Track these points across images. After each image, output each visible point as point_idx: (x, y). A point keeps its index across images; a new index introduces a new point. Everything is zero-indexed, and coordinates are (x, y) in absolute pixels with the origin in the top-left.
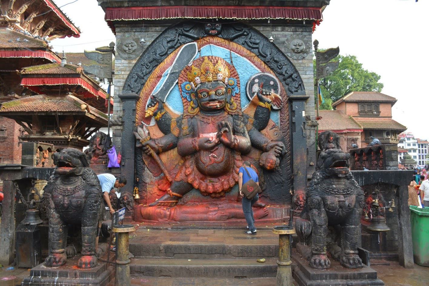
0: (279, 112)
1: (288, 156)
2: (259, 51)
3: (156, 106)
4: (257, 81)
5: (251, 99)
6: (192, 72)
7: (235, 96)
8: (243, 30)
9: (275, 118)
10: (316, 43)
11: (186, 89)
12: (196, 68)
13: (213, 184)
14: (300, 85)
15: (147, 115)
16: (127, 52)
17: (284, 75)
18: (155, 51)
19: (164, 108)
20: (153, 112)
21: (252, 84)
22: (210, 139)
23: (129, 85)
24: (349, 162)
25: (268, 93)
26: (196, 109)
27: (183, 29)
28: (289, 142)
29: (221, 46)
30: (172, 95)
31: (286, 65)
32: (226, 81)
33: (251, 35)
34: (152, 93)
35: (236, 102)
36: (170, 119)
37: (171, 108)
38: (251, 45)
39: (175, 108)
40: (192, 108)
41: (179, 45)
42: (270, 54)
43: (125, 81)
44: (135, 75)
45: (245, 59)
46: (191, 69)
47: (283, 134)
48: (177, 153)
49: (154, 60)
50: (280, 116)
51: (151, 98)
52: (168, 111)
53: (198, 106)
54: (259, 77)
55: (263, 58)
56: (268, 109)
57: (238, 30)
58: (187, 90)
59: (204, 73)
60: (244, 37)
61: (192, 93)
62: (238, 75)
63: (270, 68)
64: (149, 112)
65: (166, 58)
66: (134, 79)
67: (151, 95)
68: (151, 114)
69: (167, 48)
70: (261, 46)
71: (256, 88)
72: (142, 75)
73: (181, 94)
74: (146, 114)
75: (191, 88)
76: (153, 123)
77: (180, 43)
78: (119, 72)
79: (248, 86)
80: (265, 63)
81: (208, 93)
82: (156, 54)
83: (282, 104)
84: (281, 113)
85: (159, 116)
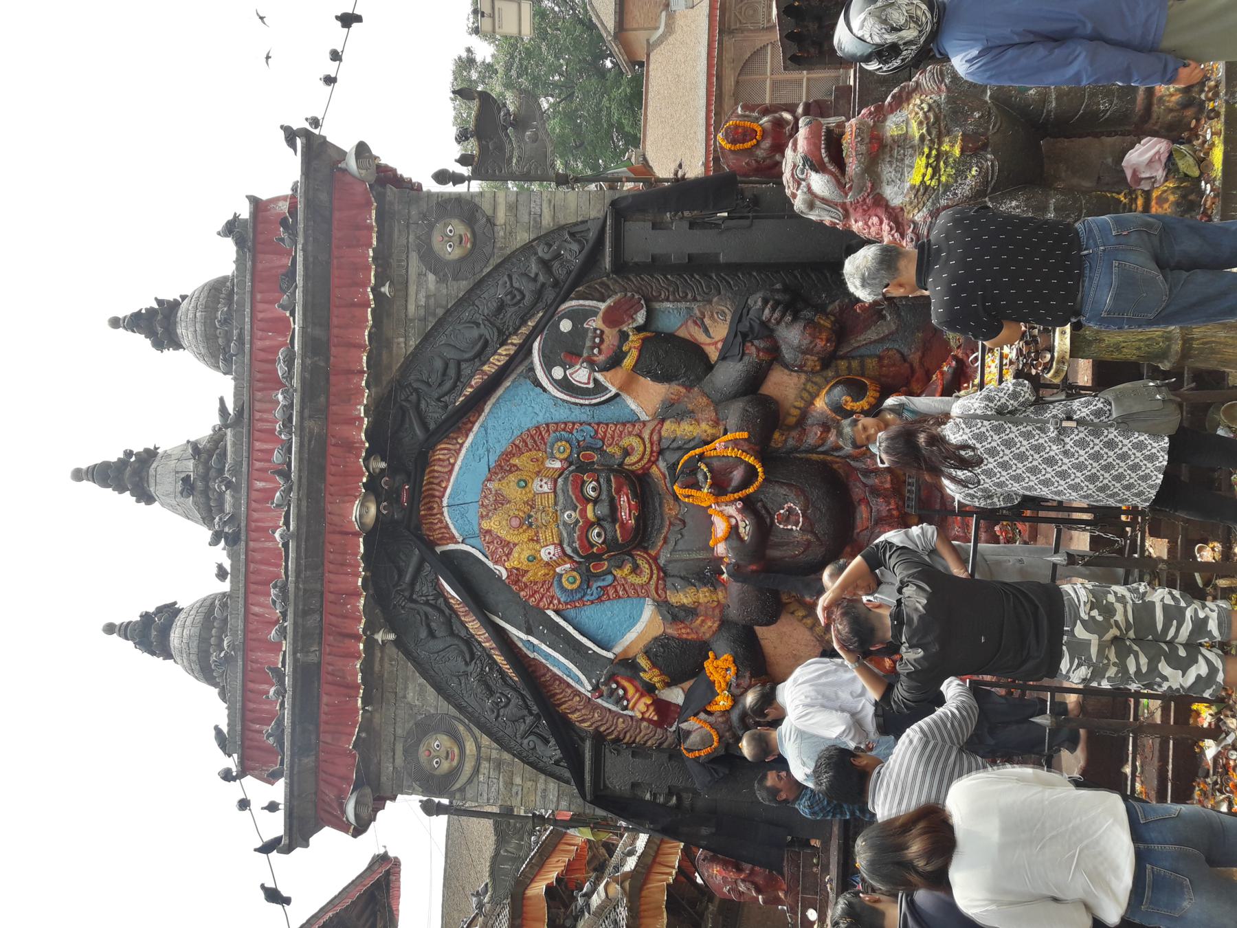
0: (657, 305)
1: (796, 277)
2: (466, 361)
3: (626, 684)
4: (558, 373)
5: (614, 391)
6: (524, 568)
7: (603, 440)
8: (402, 407)
9: (673, 317)
10: (442, 177)
11: (575, 586)
13: (876, 523)
14: (572, 235)
16: (455, 763)
17: (543, 285)
18: (458, 677)
19: (631, 655)
20: (642, 695)
21: (565, 385)
22: (733, 521)
23: (557, 763)
24: (832, 121)
25: (597, 340)
26: (639, 562)
27: (394, 586)
28: (751, 275)
29: (451, 472)
30: (591, 625)
31: (510, 277)
32: (558, 465)
33: (418, 380)
34: (582, 690)
35: (620, 436)
36: (669, 638)
37: (631, 636)
38: (448, 385)
39: (634, 621)
41: (441, 600)
42: (478, 325)
43: (543, 777)
44: (526, 741)
46: (517, 569)
47: (723, 292)
48: (772, 627)
49: (483, 680)
50: (667, 300)
52: (641, 646)
55: (489, 350)
56: (644, 340)
57: (403, 421)
58: (578, 582)
59: (531, 533)
60: (423, 402)
61: (588, 570)
62: (538, 427)
63: (519, 328)
64: (641, 707)
65: (480, 643)
66: (540, 748)
67: (589, 695)
68: (649, 702)
69: (448, 639)
70: (450, 354)
71: (581, 375)
72: (529, 720)
73: (592, 602)
74: (647, 716)
75: (575, 573)
77: (436, 599)
78: (514, 790)
79: (573, 400)
80: (502, 345)
81: (590, 525)
82: (466, 674)
83: (629, 294)
84: (657, 299)
85: (650, 675)
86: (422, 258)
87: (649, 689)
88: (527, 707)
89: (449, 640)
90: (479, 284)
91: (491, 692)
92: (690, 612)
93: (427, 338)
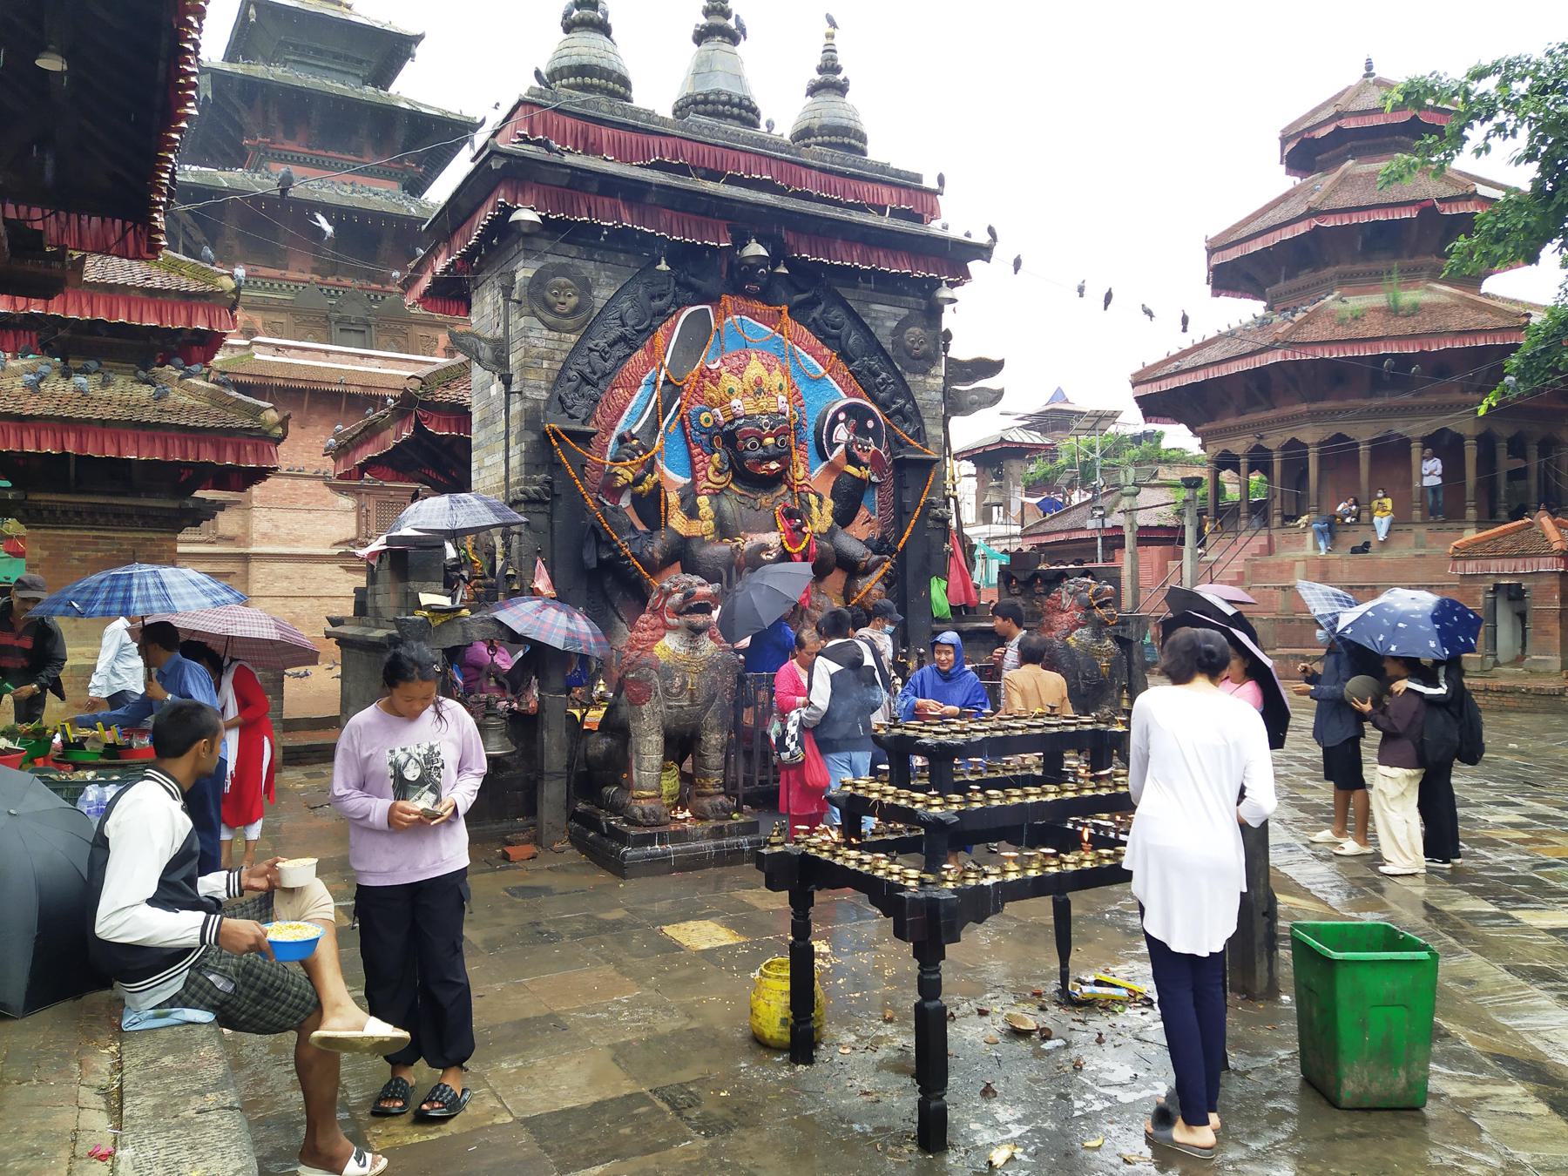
4: (842, 416)
12: (733, 378)
15: (621, 481)
18: (621, 318)
21: (835, 422)
40: (717, 470)
45: (815, 363)
49: (623, 338)
51: (622, 440)
53: (731, 467)
54: (849, 410)
59: (751, 392)
64: (625, 475)
71: (842, 434)
76: (625, 502)
81: (761, 441)
86: (906, 317)
87: (638, 481)
88: (604, 375)
89: (649, 313)
90: (888, 359)
91: (611, 345)
92: (692, 513)
93: (856, 318)
